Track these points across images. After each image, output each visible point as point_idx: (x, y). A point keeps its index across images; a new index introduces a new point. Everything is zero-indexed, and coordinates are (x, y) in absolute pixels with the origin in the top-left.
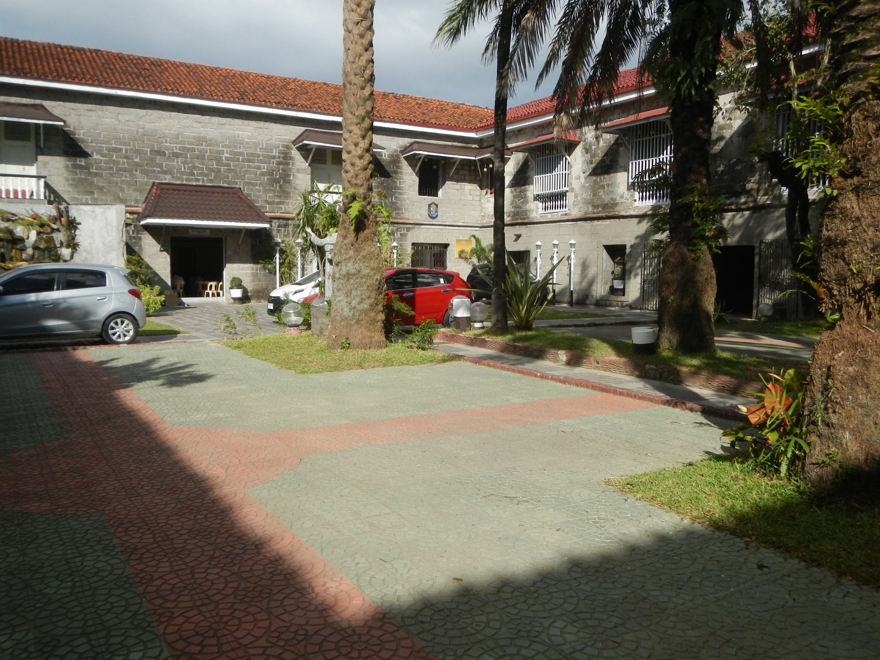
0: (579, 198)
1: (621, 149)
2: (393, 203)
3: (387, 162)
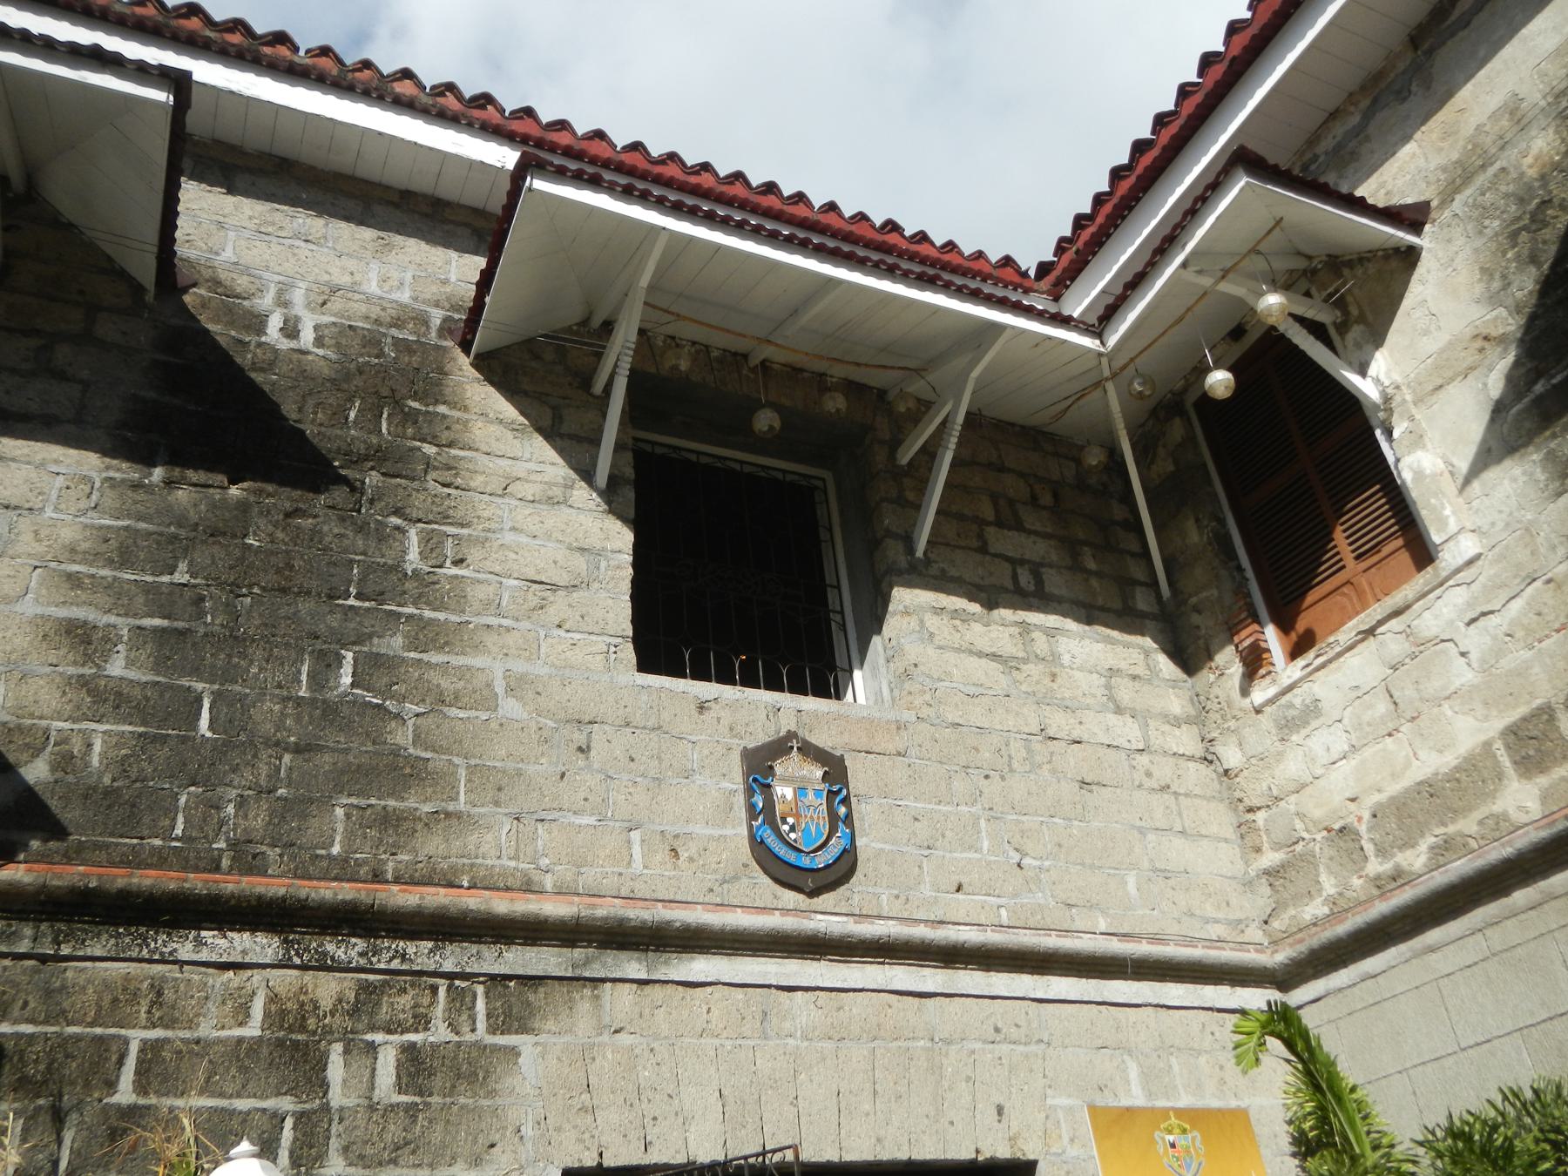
2: (331, 712)
3: (303, 374)
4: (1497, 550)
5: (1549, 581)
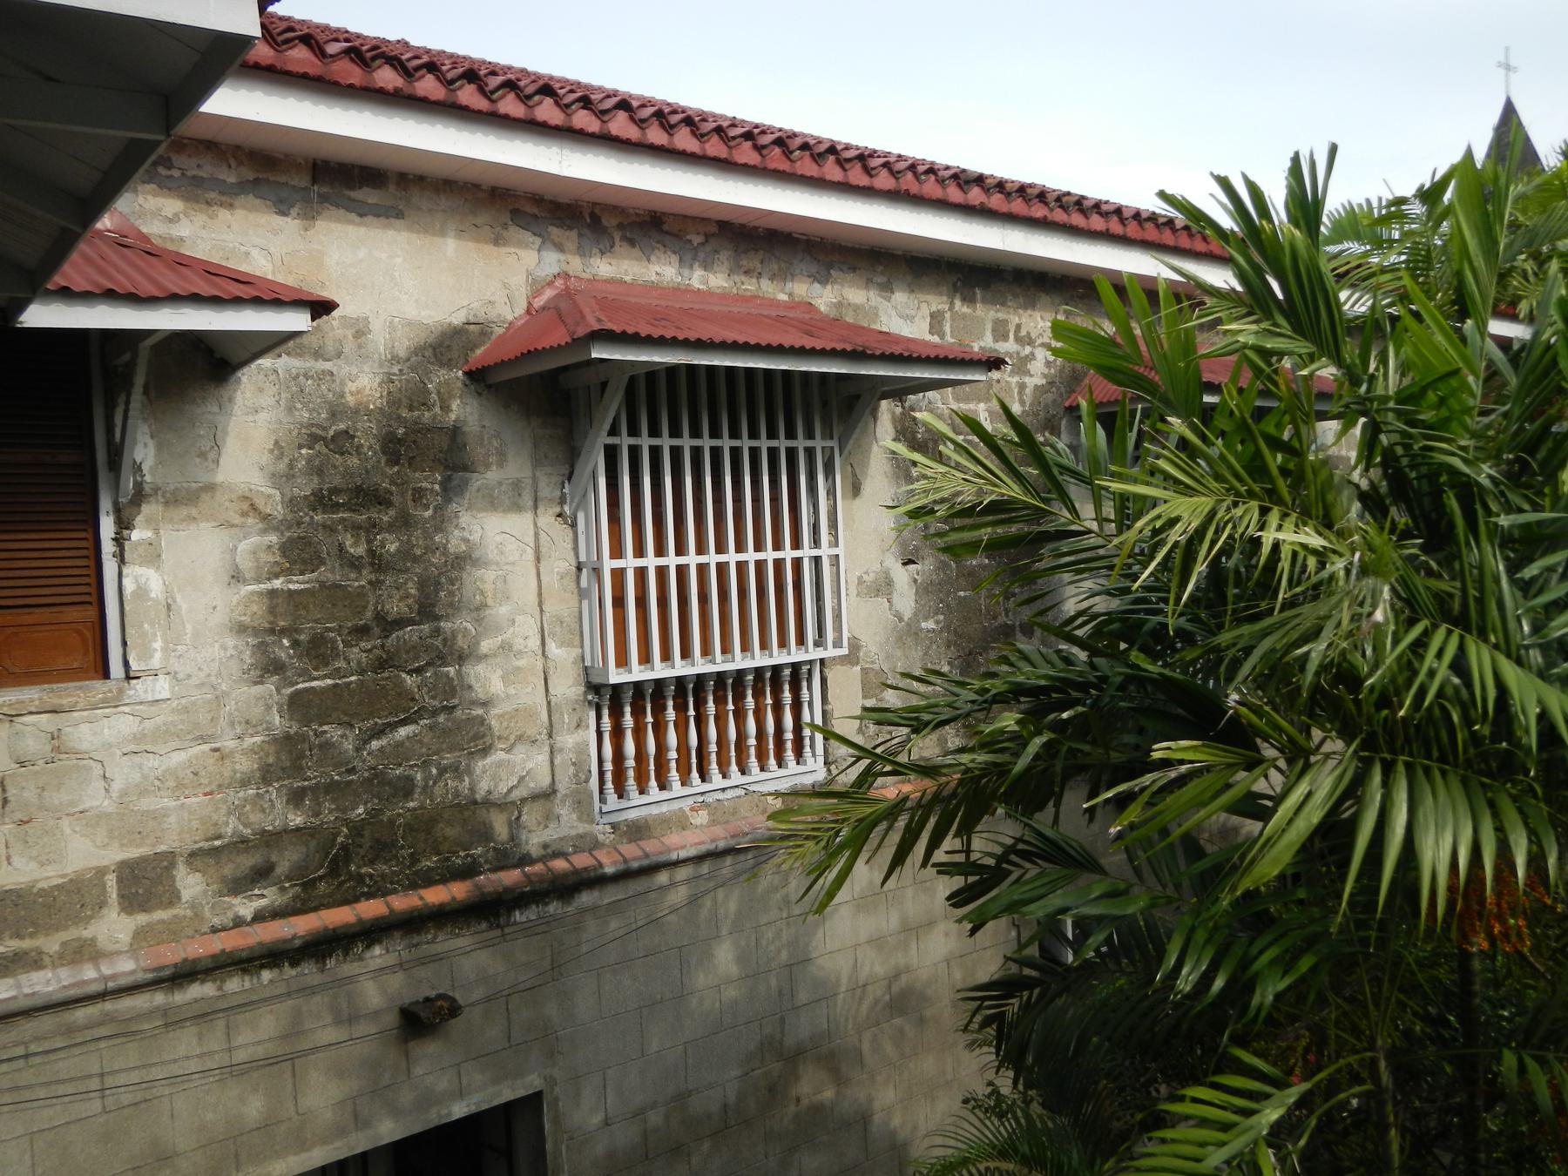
4: (184, 701)
5: (216, 750)
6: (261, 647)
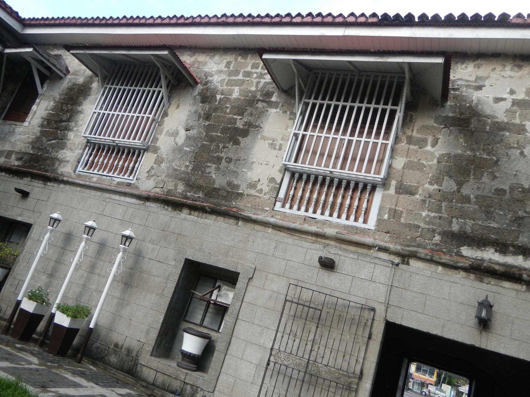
0: (163, 165)
1: (272, 111)
6: (43, 122)
